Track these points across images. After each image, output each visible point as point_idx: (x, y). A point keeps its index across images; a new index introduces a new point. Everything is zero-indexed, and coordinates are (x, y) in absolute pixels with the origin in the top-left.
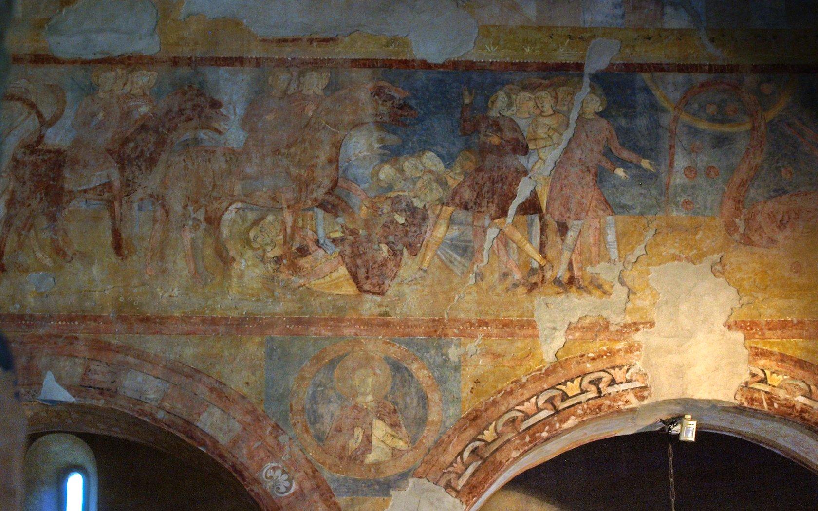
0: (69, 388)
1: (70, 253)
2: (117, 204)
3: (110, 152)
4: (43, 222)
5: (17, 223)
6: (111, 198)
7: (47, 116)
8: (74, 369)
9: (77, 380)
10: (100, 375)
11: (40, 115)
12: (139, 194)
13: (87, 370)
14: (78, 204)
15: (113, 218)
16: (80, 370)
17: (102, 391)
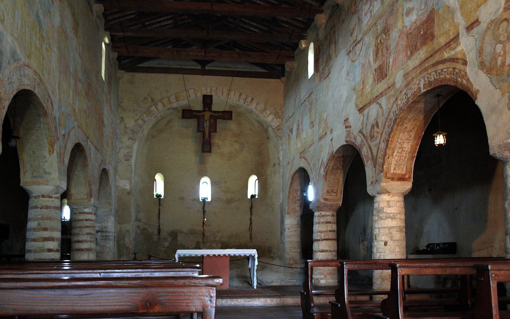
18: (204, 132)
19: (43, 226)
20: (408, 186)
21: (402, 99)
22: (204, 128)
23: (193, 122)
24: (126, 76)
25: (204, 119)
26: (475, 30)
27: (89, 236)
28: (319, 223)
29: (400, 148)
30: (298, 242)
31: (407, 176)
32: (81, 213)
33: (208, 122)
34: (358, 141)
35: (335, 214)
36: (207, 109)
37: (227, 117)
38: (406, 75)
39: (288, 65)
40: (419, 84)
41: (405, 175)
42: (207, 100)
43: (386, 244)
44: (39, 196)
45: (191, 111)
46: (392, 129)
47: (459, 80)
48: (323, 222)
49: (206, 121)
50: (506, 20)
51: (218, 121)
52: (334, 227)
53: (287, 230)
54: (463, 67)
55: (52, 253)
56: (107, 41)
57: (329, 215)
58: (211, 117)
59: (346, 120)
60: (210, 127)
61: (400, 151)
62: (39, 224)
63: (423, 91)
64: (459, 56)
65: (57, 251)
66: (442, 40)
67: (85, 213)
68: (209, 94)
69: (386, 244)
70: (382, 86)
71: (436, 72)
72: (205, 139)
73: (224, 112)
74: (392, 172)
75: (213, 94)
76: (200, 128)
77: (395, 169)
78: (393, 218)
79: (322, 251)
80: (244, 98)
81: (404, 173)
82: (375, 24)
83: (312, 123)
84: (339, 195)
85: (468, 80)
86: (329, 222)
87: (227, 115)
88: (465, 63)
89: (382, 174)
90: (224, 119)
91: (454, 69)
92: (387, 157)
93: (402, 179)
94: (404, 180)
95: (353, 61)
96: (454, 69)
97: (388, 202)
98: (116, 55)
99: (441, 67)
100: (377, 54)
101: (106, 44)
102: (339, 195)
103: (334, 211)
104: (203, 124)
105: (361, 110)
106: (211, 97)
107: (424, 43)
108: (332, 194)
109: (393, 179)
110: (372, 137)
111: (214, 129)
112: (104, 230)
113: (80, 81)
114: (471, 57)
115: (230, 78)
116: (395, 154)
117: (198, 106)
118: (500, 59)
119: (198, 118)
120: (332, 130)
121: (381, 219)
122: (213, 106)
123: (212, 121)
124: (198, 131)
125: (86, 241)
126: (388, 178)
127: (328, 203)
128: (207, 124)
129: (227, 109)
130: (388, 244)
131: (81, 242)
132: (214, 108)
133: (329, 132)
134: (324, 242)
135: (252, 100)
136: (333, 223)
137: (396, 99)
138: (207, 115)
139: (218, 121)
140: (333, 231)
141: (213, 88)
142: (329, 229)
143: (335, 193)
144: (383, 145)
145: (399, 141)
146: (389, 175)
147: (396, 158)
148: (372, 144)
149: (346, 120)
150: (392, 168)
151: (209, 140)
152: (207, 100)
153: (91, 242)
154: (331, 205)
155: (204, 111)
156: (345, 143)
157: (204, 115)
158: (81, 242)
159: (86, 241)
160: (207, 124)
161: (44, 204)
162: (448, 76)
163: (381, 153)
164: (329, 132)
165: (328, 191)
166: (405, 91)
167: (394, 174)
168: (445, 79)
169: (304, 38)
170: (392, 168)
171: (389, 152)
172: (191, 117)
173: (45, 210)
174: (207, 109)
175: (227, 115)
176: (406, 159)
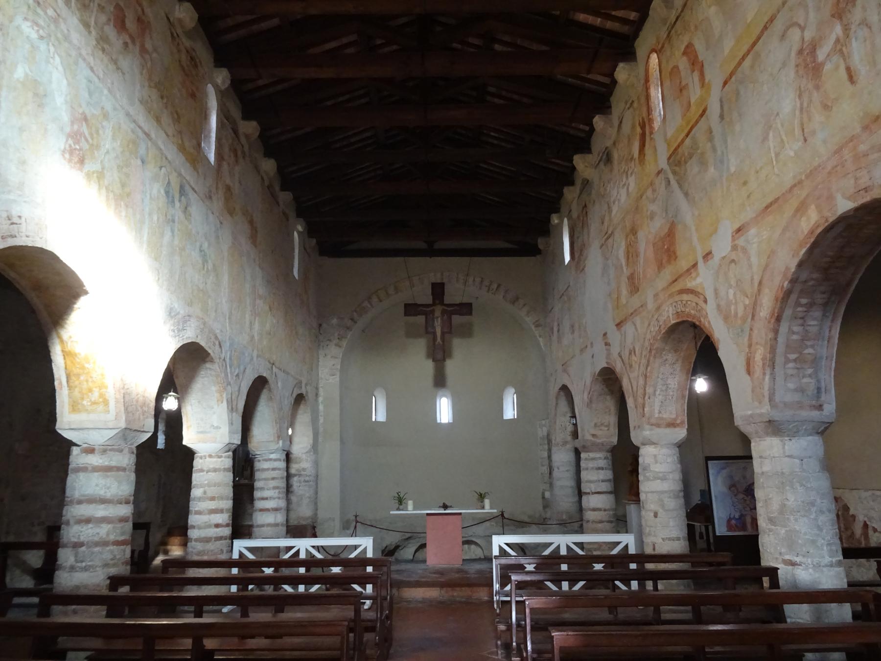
0: (849, 198)
1: (830, 104)
2: (844, 49)
3: (833, 16)
4: (815, 94)
5: (805, 105)
6: (841, 48)
7: (802, 24)
8: (849, 184)
9: (852, 191)
10: (864, 181)
11: (799, 26)
12: (853, 27)
13: (856, 179)
14: (828, 67)
15: (845, 60)
16: (852, 181)
17: (866, 190)
18: (434, 334)
19: (209, 494)
20: (681, 433)
21: (654, 326)
22: (434, 328)
24: (329, 263)
25: (434, 315)
26: (710, 262)
27: (277, 491)
28: (587, 469)
29: (663, 385)
30: (571, 487)
31: (678, 422)
32: (266, 460)
34: (618, 367)
35: (609, 455)
38: (656, 295)
39: (541, 242)
40: (668, 311)
41: (675, 419)
42: (438, 290)
43: (656, 515)
44: (205, 456)
45: (416, 305)
46: (648, 361)
47: (702, 320)
48: (592, 468)
50: (733, 261)
52: (609, 474)
53: (556, 469)
54: (703, 305)
55: (220, 529)
56: (300, 228)
57: (600, 458)
58: (444, 312)
59: (605, 334)
61: (664, 388)
62: (205, 493)
63: (673, 322)
64: (699, 290)
65: (227, 525)
66: (683, 264)
67: (271, 460)
68: (439, 281)
69: (656, 515)
70: (635, 301)
71: (682, 301)
73: (461, 305)
74: (657, 415)
77: (660, 412)
78: (664, 479)
79: (594, 510)
80: (488, 284)
81: (674, 416)
82: (623, 218)
83: (572, 326)
84: (612, 429)
85: (709, 322)
86: (602, 469)
87: (466, 308)
88: (706, 301)
89: (644, 419)
91: (697, 304)
92: (647, 398)
93: (672, 425)
94: (675, 427)
95: (607, 259)
96: (697, 304)
97: (655, 456)
98: (314, 241)
99: (685, 297)
100: (628, 258)
101: (299, 232)
102: (612, 429)
103: (608, 451)
105: (619, 325)
107: (669, 262)
108: (603, 428)
109: (658, 426)
110: (631, 366)
112: (302, 473)
113: (260, 297)
114: (710, 294)
115: (468, 258)
116: (658, 393)
117: (426, 298)
118: (733, 307)
120: (592, 343)
121: (648, 479)
123: (445, 317)
124: (427, 332)
125: (271, 498)
126: (652, 425)
127: (598, 441)
129: (465, 300)
130: (659, 515)
131: (266, 499)
132: (447, 300)
133: (589, 346)
134: (596, 495)
135: (499, 286)
136: (606, 469)
137: (649, 325)
140: (609, 480)
142: (601, 477)
143: (606, 426)
144: (641, 382)
145: (661, 376)
146: (653, 421)
147: (660, 397)
148: (632, 375)
149: (605, 334)
150: (656, 411)
152: (438, 290)
153: (279, 498)
154: (603, 444)
155: (434, 304)
156: (606, 366)
158: (266, 499)
159: (271, 498)
161: (212, 466)
162: (692, 312)
163: (640, 391)
164: (589, 346)
165: (595, 424)
166: (656, 317)
167: (662, 419)
168: (689, 315)
169: (557, 210)
170: (656, 411)
171: (649, 390)
173: (213, 474)
174: (437, 302)
176: (674, 398)
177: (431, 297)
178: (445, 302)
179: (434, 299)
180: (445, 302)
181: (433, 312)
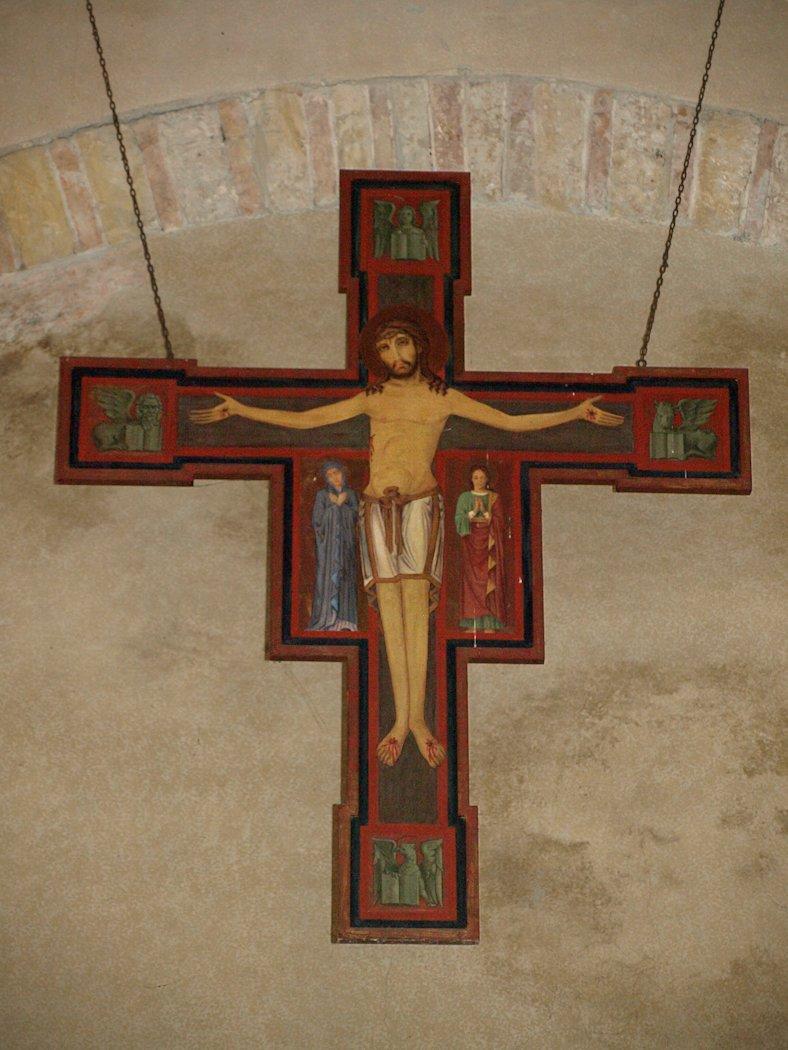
22: (362, 600)
23: (204, 539)
25: (358, 476)
33: (416, 518)
36: (397, 352)
37: (669, 447)
45: (180, 378)
49: (394, 503)
51: (563, 508)
58: (456, 456)
60: (446, 598)
68: (416, 153)
72: (386, 752)
75: (475, 160)
76: (306, 606)
87: (679, 425)
90: (636, 473)
104: (355, 555)
106: (449, 194)
111: (498, 604)
119: (287, 471)
122: (473, 306)
123: (477, 501)
124: (289, 637)
128: (402, 555)
138: (406, 423)
139: (563, 508)
141: (471, 98)
151: (432, 752)
152: (404, 245)
155: (367, 371)
157: (362, 422)
160: (402, 555)
172: (179, 464)
174: (397, 352)
175: (679, 425)
177: (335, 311)
178: (478, 359)
179: (363, 329)
180: (478, 359)
181: (352, 448)
